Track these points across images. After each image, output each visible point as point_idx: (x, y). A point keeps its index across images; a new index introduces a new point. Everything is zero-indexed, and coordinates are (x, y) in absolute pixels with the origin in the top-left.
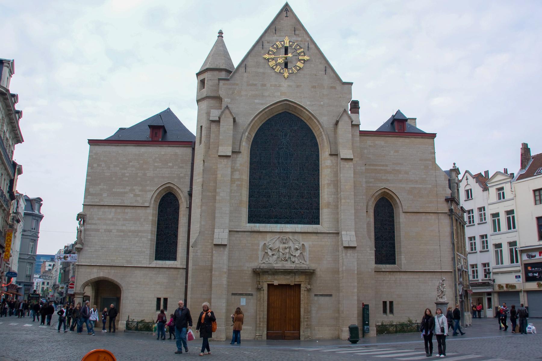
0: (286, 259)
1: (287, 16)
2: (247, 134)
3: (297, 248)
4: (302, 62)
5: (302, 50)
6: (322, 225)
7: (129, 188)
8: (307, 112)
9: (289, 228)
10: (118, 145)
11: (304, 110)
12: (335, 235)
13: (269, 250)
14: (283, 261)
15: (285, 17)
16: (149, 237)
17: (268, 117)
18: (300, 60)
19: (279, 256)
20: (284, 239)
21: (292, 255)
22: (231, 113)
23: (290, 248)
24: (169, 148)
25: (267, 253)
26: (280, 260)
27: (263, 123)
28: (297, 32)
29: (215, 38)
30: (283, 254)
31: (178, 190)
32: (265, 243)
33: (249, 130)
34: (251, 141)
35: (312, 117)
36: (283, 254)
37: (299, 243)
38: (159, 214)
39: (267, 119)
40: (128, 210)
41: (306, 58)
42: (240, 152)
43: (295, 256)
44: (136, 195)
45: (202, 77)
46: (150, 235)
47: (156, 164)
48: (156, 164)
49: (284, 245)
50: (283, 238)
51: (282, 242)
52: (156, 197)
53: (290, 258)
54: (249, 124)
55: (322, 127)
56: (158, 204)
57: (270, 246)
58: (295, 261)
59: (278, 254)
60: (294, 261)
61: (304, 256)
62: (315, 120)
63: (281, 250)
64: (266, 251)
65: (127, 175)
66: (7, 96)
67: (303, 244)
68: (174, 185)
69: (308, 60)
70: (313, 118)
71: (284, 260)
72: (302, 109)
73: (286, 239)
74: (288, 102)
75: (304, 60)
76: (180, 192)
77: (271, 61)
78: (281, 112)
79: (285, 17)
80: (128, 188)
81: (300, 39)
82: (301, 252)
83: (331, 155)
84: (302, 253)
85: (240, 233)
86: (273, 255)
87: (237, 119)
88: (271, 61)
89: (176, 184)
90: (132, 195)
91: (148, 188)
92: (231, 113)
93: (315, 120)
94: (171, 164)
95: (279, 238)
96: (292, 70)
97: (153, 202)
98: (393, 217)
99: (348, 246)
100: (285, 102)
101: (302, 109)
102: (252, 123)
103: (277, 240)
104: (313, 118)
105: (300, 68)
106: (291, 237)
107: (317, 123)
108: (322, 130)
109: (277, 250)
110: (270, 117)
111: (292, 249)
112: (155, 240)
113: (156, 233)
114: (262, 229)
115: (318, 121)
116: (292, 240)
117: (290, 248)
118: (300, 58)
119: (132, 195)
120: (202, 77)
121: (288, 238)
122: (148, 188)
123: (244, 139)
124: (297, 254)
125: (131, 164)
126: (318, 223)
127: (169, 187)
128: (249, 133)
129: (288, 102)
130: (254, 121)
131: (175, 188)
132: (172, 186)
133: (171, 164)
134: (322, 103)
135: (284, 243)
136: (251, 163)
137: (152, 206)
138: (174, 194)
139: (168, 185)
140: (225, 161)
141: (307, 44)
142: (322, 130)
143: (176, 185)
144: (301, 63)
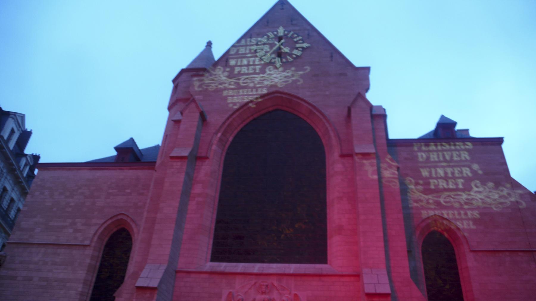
1: (282, 9)
2: (219, 135)
4: (300, 49)
5: (300, 38)
6: (330, 264)
7: (70, 221)
8: (306, 105)
9: (275, 268)
10: (70, 170)
11: (303, 103)
12: (352, 279)
15: (281, 9)
16: (80, 289)
17: (252, 115)
18: (297, 48)
20: (263, 285)
22: (197, 107)
24: (131, 171)
27: (245, 123)
28: (294, 22)
29: (202, 47)
31: (131, 223)
33: (222, 130)
34: (227, 146)
35: (313, 110)
38: (103, 257)
39: (251, 118)
40: (62, 251)
41: (305, 45)
42: (206, 158)
44: (76, 231)
45: (176, 82)
46: (81, 285)
47: (111, 191)
48: (111, 191)
50: (262, 284)
52: (102, 233)
54: (224, 123)
55: (328, 121)
56: (104, 243)
57: (239, 297)
62: (317, 113)
65: (72, 204)
66: (5, 150)
67: (296, 295)
68: (128, 216)
69: (308, 48)
70: (315, 111)
72: (299, 101)
73: (267, 286)
74: (279, 95)
75: (303, 48)
76: (133, 226)
77: (260, 52)
78: (271, 109)
79: (281, 9)
80: (70, 221)
81: (297, 28)
83: (342, 156)
85: (193, 275)
87: (208, 118)
88: (260, 52)
89: (130, 216)
90: (71, 231)
91: (94, 221)
92: (197, 107)
93: (317, 113)
94: (128, 191)
96: (287, 59)
97: (96, 238)
98: (454, 261)
99: (373, 291)
100: (276, 95)
101: (299, 101)
102: (229, 122)
104: (315, 111)
105: (297, 56)
106: (276, 283)
107: (321, 117)
108: (327, 125)
110: (255, 116)
112: (90, 295)
113: (93, 285)
114: (227, 270)
115: (323, 115)
118: (298, 45)
119: (71, 231)
120: (176, 82)
122: (94, 221)
123: (215, 140)
125: (80, 191)
126: (326, 263)
127: (122, 219)
128: (223, 135)
129: (279, 95)
130: (231, 119)
131: (129, 220)
132: (124, 218)
133: (128, 191)
134: (327, 93)
135: (263, 293)
136: (224, 176)
137: (93, 244)
138: (128, 231)
139: (119, 217)
140: (177, 164)
141: (306, 32)
142: (327, 125)
143: (130, 217)
144: (300, 51)
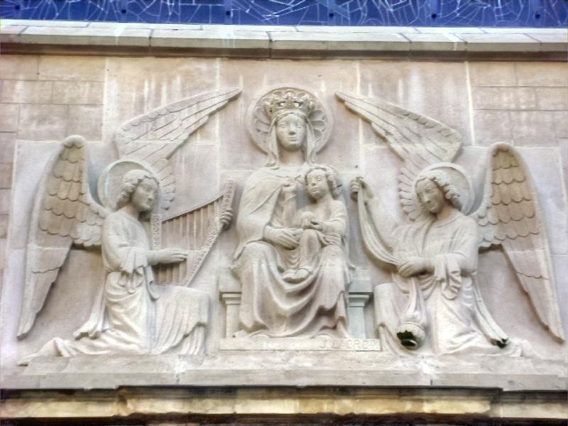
0: (326, 301)
3: (442, 189)
13: (123, 219)
14: (283, 331)
19: (235, 275)
21: (389, 269)
23: (356, 196)
25: (96, 250)
26: (249, 315)
30: (287, 249)
32: (73, 146)
36: (287, 249)
37: (452, 149)
43: (423, 273)
49: (293, 171)
51: (272, 146)
53: (370, 301)
58: (427, 329)
59: (220, 261)
60: (415, 329)
61: (529, 285)
63: (253, 218)
64: (86, 234)
71: (298, 315)
82: (491, 235)
84: (497, 248)
86: (163, 268)
95: (234, 99)
103: (216, 127)
106: (364, 101)
109: (217, 218)
111: (386, 206)
116: (377, 124)
117: (356, 196)
121: (329, 111)
124: (451, 247)
135: (286, 150)
